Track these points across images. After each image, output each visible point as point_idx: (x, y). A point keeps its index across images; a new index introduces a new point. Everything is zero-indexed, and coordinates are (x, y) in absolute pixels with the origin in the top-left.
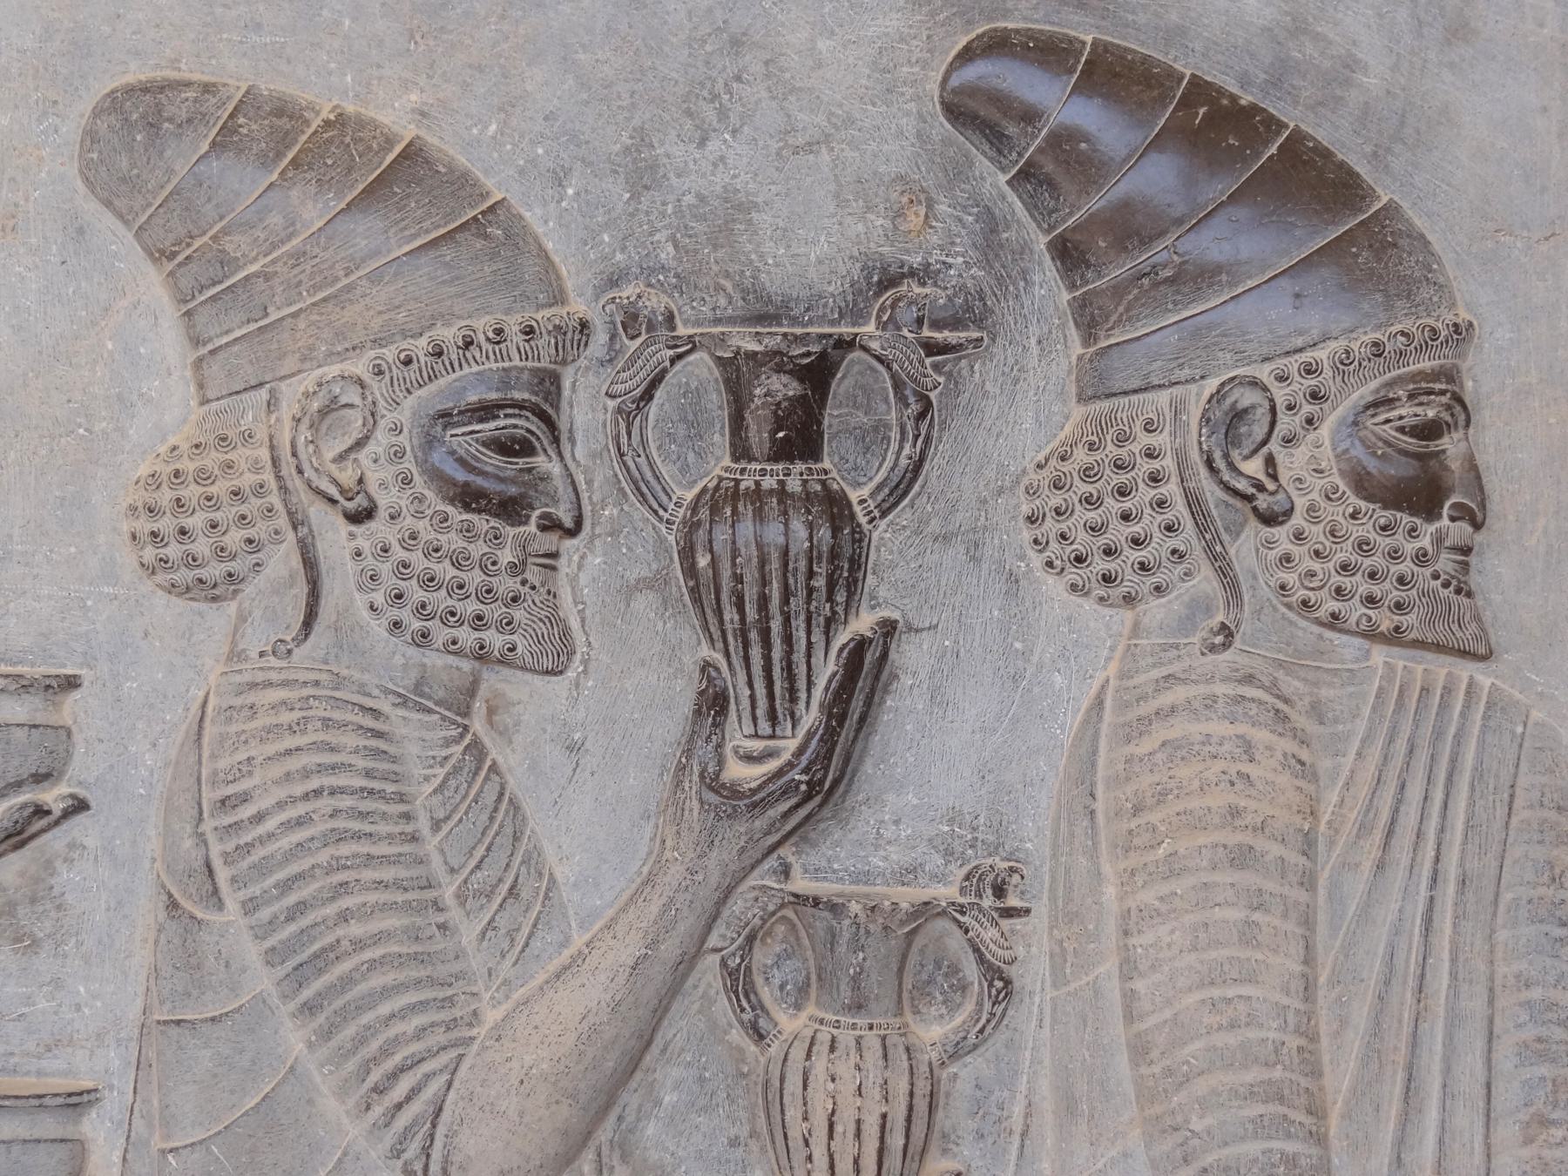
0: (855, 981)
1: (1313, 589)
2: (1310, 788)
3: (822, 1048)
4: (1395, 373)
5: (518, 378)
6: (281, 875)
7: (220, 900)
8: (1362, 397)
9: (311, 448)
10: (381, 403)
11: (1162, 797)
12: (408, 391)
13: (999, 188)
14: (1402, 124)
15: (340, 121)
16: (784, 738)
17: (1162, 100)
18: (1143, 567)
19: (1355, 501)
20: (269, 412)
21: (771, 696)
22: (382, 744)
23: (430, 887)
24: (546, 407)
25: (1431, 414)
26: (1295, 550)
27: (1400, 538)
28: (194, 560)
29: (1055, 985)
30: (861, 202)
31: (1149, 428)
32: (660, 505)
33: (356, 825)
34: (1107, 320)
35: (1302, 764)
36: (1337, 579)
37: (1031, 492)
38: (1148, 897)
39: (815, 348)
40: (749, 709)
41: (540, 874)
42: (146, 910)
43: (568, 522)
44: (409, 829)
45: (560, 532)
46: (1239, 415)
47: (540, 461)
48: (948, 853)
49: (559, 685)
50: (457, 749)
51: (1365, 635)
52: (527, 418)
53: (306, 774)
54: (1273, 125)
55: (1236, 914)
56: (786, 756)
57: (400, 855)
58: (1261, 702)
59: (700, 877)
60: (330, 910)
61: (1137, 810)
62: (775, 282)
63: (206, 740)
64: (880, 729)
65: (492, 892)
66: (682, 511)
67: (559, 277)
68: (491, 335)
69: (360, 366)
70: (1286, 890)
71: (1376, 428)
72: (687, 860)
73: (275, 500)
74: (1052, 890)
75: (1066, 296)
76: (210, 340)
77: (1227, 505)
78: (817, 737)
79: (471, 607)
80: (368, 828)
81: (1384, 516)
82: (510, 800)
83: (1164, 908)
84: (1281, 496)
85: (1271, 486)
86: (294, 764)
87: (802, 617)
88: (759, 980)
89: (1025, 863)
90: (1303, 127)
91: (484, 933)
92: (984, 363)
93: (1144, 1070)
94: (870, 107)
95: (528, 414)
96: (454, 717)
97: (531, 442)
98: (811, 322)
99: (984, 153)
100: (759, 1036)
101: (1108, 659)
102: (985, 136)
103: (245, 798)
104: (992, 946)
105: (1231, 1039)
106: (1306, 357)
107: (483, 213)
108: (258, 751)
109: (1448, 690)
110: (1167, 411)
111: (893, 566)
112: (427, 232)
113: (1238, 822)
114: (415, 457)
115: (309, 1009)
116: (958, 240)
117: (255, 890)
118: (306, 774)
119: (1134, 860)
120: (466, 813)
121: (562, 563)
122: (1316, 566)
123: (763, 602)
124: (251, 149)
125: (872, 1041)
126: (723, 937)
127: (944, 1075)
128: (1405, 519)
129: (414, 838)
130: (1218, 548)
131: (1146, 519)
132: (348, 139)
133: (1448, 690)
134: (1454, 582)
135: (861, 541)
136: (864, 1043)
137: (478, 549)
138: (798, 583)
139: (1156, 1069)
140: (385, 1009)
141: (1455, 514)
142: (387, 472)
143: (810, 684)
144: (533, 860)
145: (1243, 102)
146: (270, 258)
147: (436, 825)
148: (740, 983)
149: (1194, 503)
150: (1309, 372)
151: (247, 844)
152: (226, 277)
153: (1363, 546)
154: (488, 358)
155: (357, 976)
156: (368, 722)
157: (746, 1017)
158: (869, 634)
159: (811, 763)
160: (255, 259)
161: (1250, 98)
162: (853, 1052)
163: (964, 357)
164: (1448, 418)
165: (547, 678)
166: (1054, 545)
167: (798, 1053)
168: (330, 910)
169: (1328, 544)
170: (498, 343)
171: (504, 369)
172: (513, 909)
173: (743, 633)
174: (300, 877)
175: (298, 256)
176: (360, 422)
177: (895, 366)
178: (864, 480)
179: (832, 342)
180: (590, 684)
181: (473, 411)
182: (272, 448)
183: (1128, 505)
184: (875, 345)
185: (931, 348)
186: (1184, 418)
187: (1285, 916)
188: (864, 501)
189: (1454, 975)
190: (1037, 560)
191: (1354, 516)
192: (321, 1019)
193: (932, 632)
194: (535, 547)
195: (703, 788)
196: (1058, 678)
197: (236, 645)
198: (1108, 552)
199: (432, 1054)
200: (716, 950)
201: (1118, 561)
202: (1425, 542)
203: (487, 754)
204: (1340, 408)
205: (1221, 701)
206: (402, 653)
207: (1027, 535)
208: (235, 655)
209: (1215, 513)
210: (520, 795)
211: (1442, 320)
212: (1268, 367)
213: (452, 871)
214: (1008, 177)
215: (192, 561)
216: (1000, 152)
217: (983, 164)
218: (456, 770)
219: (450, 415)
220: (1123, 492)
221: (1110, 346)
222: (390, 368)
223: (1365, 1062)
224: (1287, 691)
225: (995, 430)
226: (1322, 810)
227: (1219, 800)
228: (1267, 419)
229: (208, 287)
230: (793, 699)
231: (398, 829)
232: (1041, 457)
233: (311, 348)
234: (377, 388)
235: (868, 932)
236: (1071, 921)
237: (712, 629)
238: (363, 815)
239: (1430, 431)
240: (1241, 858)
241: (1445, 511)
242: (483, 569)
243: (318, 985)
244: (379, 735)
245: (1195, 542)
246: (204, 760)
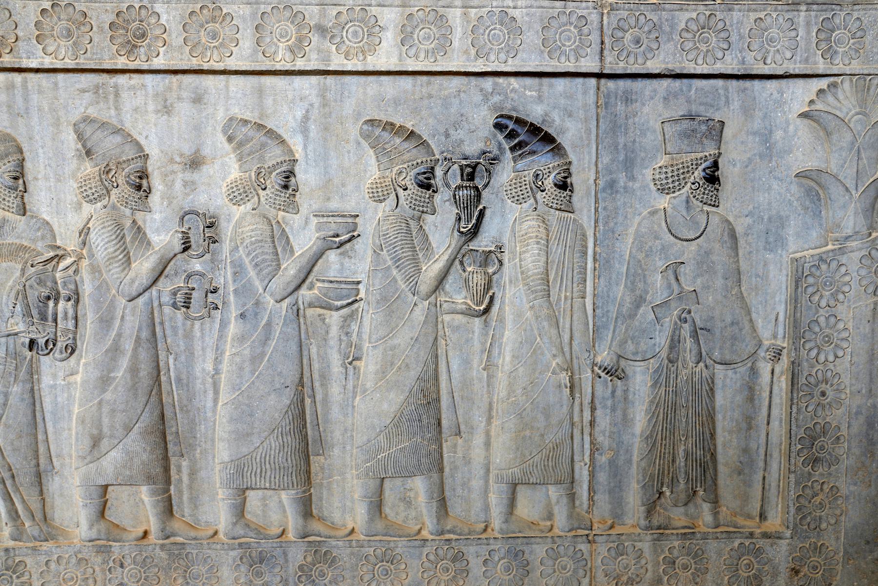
3: (475, 273)
11: (526, 234)
19: (555, 188)
27: (561, 194)
42: (370, 252)
46: (538, 175)
49: (434, 216)
53: (397, 230)
61: (522, 236)
62: (467, 153)
69: (405, 166)
73: (392, 187)
79: (422, 204)
81: (559, 191)
86: (395, 229)
100: (464, 271)
103: (388, 234)
105: (536, 271)
115: (398, 267)
118: (397, 230)
119: (522, 244)
123: (467, 203)
138: (472, 200)
144: (430, 244)
148: (462, 263)
149: (531, 188)
167: (471, 274)
173: (464, 208)
175: (396, 148)
185: (491, 164)
190: (506, 197)
206: (411, 211)
207: (505, 193)
208: (384, 211)
211: (568, 161)
215: (379, 196)
217: (499, 135)
220: (521, 187)
227: (534, 234)
239: (566, 178)
240: (538, 243)
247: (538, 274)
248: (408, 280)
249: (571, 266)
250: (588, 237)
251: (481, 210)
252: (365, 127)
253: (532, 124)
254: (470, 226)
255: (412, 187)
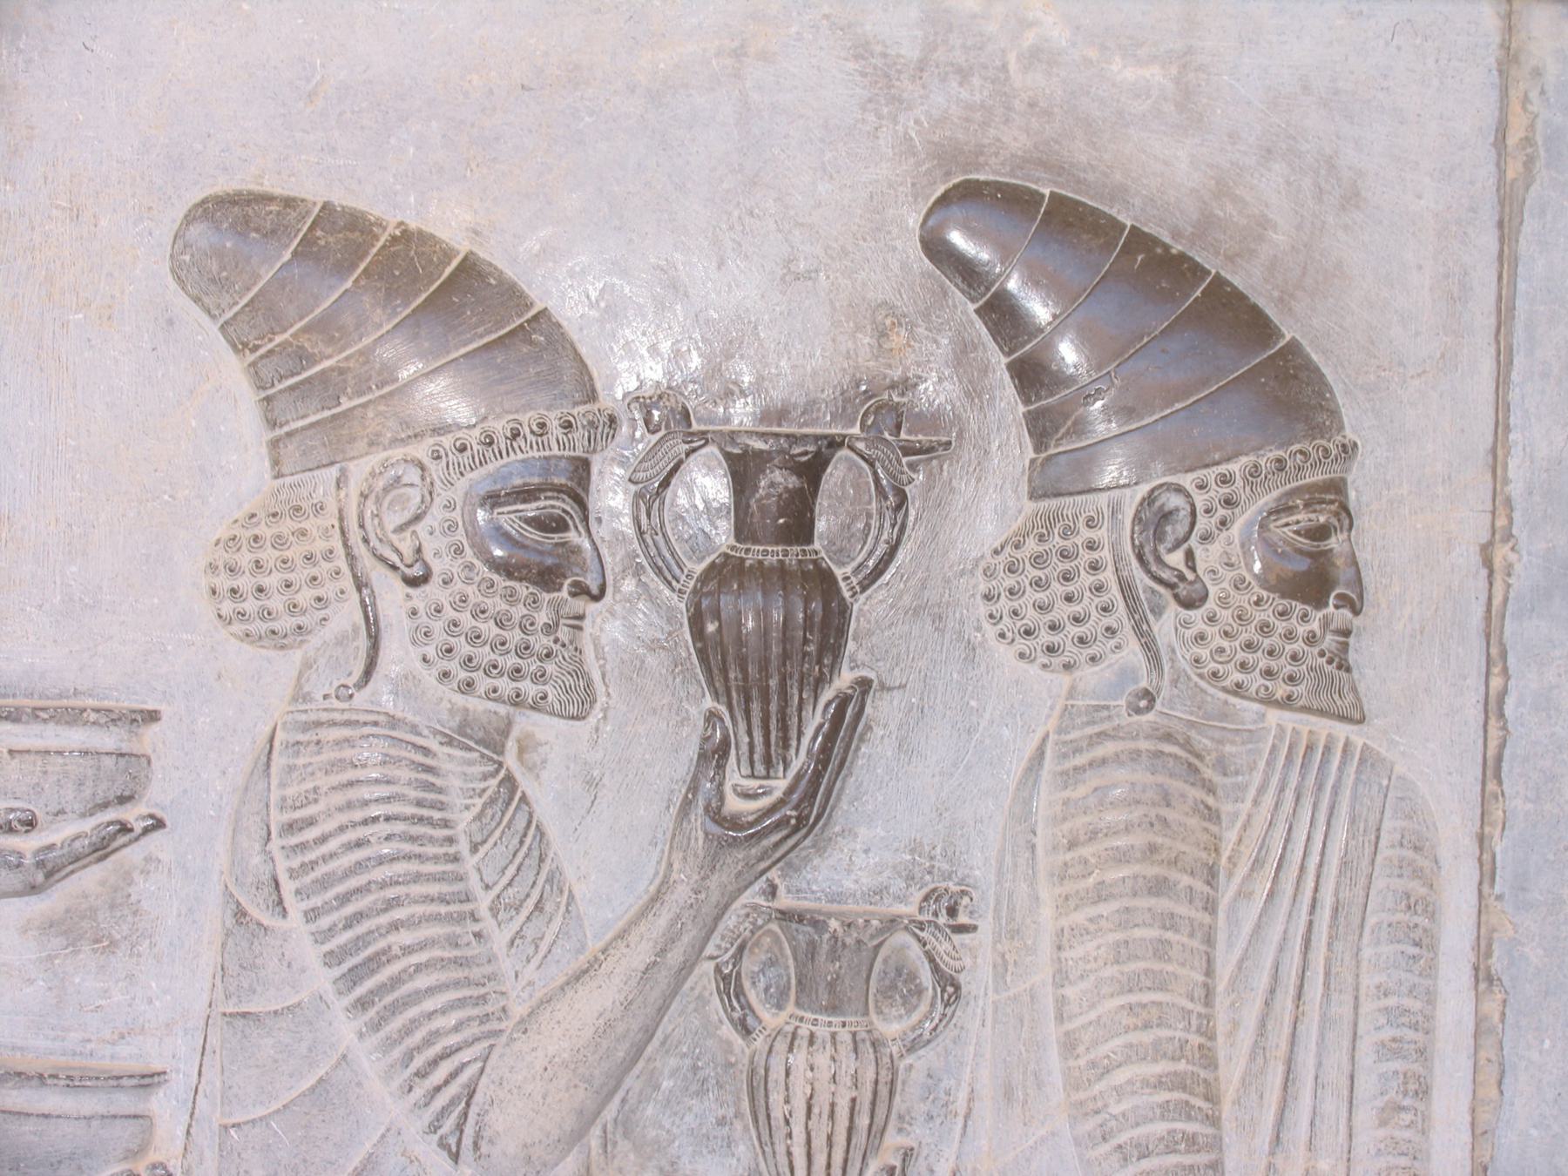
0: (831, 986)
1: (1221, 663)
2: (1214, 829)
4: (1294, 484)
5: (556, 466)
6: (340, 889)
7: (284, 909)
8: (1266, 504)
9: (376, 521)
10: (438, 483)
12: (462, 474)
13: (968, 315)
14: (1304, 274)
15: (406, 236)
16: (777, 778)
17: (1108, 246)
18: (1082, 640)
20: (338, 487)
21: (767, 743)
22: (431, 778)
23: (468, 900)
24: (580, 491)
25: (1322, 519)
26: (1210, 630)
28: (269, 614)
29: (996, 991)
30: (851, 324)
31: (1091, 523)
32: (674, 577)
33: (407, 847)
34: (1057, 430)
35: (1208, 808)
36: (1241, 656)
37: (989, 573)
38: (1079, 917)
39: (811, 448)
40: (747, 754)
41: (561, 892)
42: (214, 916)
43: (595, 590)
44: (451, 850)
45: (586, 597)
46: (1166, 516)
47: (572, 536)
48: (910, 878)
49: (583, 728)
50: (493, 782)
51: (1261, 701)
52: (564, 501)
54: (1198, 271)
55: (1154, 933)
56: (778, 794)
57: (444, 872)
58: (1176, 757)
59: (702, 896)
60: (384, 919)
61: (1072, 845)
63: (274, 770)
64: (856, 771)
65: (521, 906)
66: (692, 583)
67: (591, 379)
68: (535, 428)
69: (421, 451)
70: (1193, 914)
71: (1278, 530)
72: (692, 882)
74: (997, 910)
75: (1021, 409)
76: (287, 422)
77: (1153, 591)
78: (807, 777)
79: (511, 661)
80: (417, 849)
82: (537, 826)
83: (1092, 928)
84: (1198, 586)
85: (1190, 576)
87: (796, 676)
88: (747, 984)
89: (975, 888)
90: (1223, 273)
91: (512, 942)
92: (951, 465)
93: (1071, 1063)
94: (861, 242)
95: (565, 497)
96: (491, 754)
97: (565, 520)
98: (806, 424)
99: (956, 285)
100: (746, 1031)
101: (1048, 717)
102: (958, 271)
103: (311, 822)
104: (945, 957)
105: (1147, 1037)
106: (1222, 469)
107: (528, 321)
108: (324, 782)
109: (1328, 749)
110: (1105, 510)
111: (870, 633)
112: (481, 336)
113: (1156, 857)
114: (466, 531)
115: (363, 1004)
116: (932, 358)
117: (316, 901)
119: (1069, 887)
120: (501, 838)
121: (586, 624)
122: (1225, 644)
124: (328, 259)
125: (844, 1036)
126: (719, 947)
127: (902, 1065)
128: (1299, 607)
129: (456, 859)
130: (1145, 627)
131: (1086, 601)
132: (412, 253)
133: (1328, 749)
134: (1337, 660)
135: (845, 612)
136: (838, 1038)
137: (519, 611)
139: (1082, 1062)
140: (429, 1005)
141: (1340, 603)
142: (441, 543)
143: (800, 734)
145: (1174, 251)
146: (344, 355)
147: (475, 848)
148: (730, 986)
149: (1126, 588)
150: (1224, 482)
151: (311, 862)
152: (303, 369)
153: (1265, 629)
154: (531, 447)
155: (405, 977)
156: (420, 758)
157: (736, 1015)
158: (850, 691)
159: (801, 801)
160: (329, 357)
161: (1180, 248)
162: (828, 1046)
163: (935, 458)
164: (1337, 524)
165: (571, 722)
166: (1006, 619)
168: (384, 919)
169: (1235, 625)
170: (541, 435)
171: (545, 458)
172: (538, 921)
174: (358, 891)
176: (418, 499)
177: (877, 464)
178: (846, 560)
179: (825, 442)
180: (608, 728)
181: (518, 493)
182: (341, 519)
183: (1071, 589)
184: (861, 446)
186: (1120, 517)
187: (1191, 935)
188: (848, 578)
189: (1327, 985)
190: (991, 631)
191: (1257, 603)
192: (372, 1013)
193: (901, 691)
194: (565, 610)
195: (708, 820)
196: (1006, 732)
197: (301, 688)
198: (1053, 627)
199: (469, 1044)
200: (712, 958)
201: (1061, 635)
202: (1315, 626)
203: (517, 788)
204: (1249, 512)
205: (1144, 755)
207: (983, 609)
208: (300, 696)
209: (1142, 597)
210: (545, 822)
212: (1191, 476)
213: (487, 887)
214: (976, 306)
216: (970, 286)
218: (492, 801)
219: (499, 496)
220: (1066, 577)
221: (1059, 453)
222: (447, 455)
223: (1253, 1057)
224: (1198, 747)
225: (960, 521)
226: (1223, 846)
227: (1138, 839)
228: (1187, 521)
229: (287, 377)
230: (786, 746)
231: (441, 851)
232: (997, 544)
233: (378, 435)
234: (436, 470)
235: (844, 945)
236: (1012, 938)
237: (717, 685)
238: (412, 839)
239: (1320, 533)
240: (1159, 887)
241: (1331, 601)
242: (523, 629)
243: (369, 984)
244: (429, 769)
245: (1125, 621)
246: (272, 787)
247: (1157, 1052)
248: (421, 1074)
249: (1342, 1008)
250: (1445, 854)
251: (843, 701)
252: (199, 233)
253: (1140, 240)
254: (780, 785)
255: (457, 569)
